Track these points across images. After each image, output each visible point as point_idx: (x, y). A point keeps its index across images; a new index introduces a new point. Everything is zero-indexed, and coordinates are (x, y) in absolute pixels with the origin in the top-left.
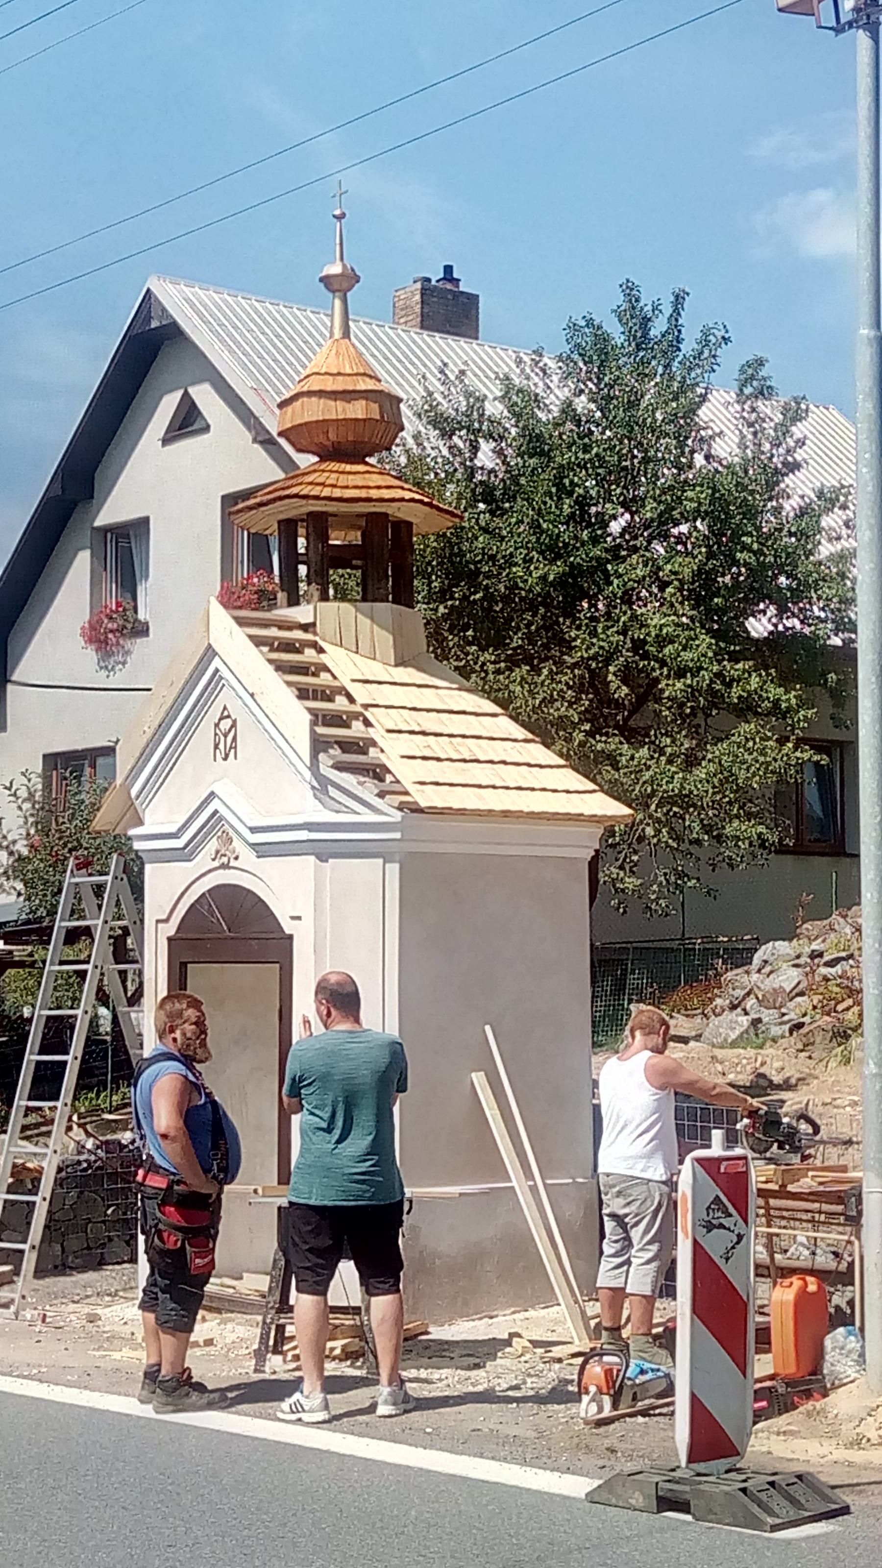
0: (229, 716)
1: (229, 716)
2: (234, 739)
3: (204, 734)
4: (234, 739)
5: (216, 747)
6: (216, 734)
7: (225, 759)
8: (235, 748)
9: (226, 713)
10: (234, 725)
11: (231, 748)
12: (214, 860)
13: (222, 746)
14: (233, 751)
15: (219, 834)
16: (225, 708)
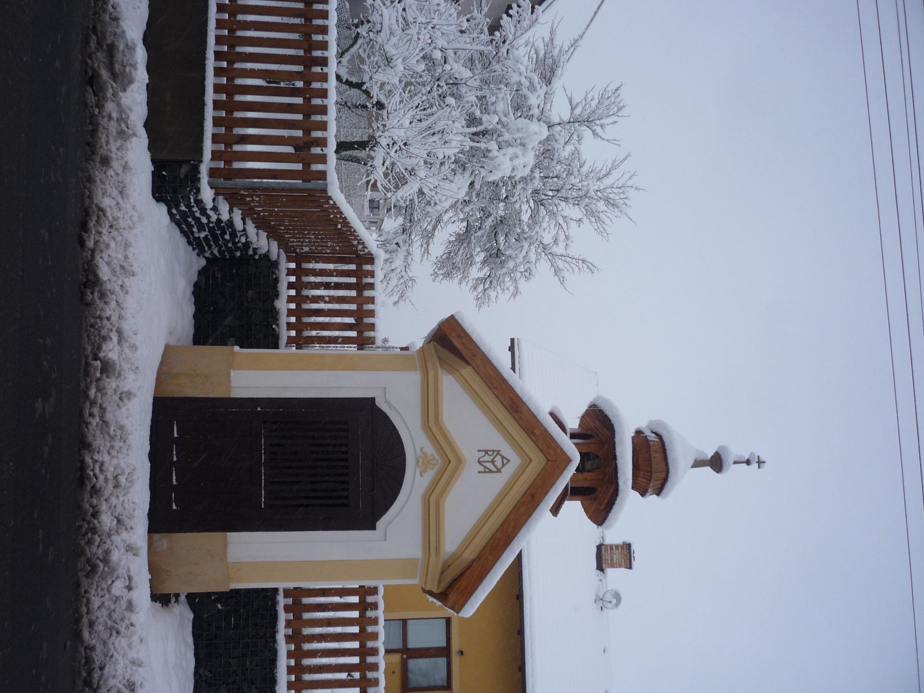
0: (503, 465)
1: (503, 465)
2: (491, 471)
3: (497, 441)
4: (491, 471)
5: (486, 452)
6: (493, 451)
7: (480, 462)
8: (485, 472)
9: (505, 461)
10: (499, 471)
11: (485, 467)
12: (421, 449)
13: (488, 458)
14: (482, 469)
15: (437, 457)
16: (508, 461)
